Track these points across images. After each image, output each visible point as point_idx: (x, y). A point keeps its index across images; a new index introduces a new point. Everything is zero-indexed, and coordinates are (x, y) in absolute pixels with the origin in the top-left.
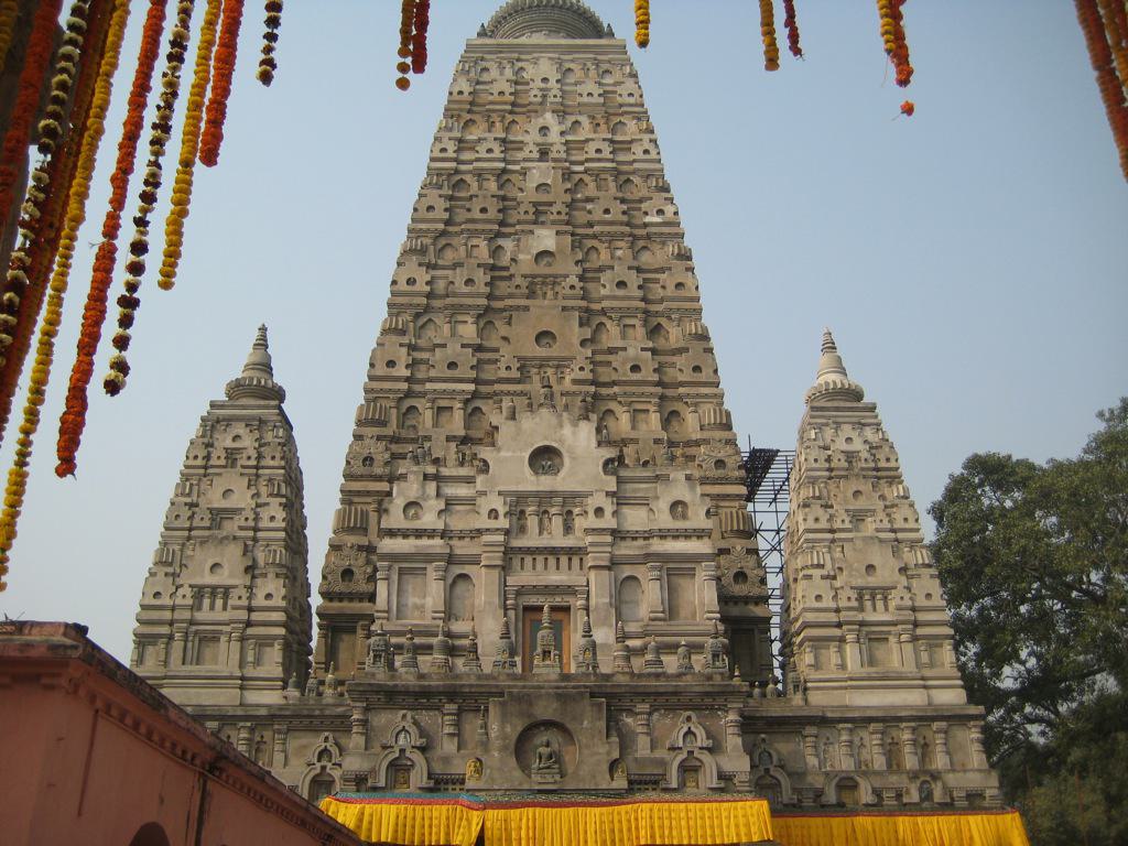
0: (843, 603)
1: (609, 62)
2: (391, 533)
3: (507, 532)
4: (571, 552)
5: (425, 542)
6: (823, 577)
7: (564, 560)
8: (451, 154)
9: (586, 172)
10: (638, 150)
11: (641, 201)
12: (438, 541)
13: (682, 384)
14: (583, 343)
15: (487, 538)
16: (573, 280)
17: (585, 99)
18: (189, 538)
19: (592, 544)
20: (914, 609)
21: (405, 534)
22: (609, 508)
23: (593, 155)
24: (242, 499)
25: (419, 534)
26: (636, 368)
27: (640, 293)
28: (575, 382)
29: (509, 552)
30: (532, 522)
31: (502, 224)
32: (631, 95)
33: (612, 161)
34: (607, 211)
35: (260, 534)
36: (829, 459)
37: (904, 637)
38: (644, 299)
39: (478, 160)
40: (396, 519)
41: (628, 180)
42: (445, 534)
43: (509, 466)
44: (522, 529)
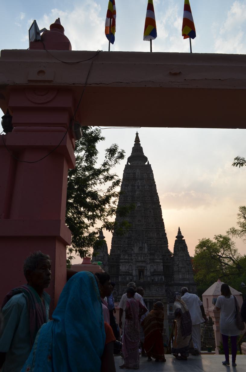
0: (179, 269)
1: (148, 169)
2: (121, 259)
3: (136, 259)
4: (144, 262)
5: (126, 260)
6: (177, 265)
7: (143, 263)
8: (124, 188)
9: (145, 191)
10: (153, 187)
11: (153, 196)
12: (127, 260)
13: (160, 229)
14: (145, 222)
15: (134, 260)
16: (143, 211)
17: (144, 177)
18: (95, 260)
19: (147, 261)
20: (188, 270)
21: (123, 259)
22: (149, 256)
23: (146, 188)
24: (102, 255)
25: (125, 259)
26: (152, 226)
27: (153, 213)
28: (144, 228)
29: (136, 261)
30: (139, 257)
31: (132, 201)
32: (152, 176)
33: (149, 189)
34: (148, 199)
35: (105, 260)
36: (178, 248)
37: (187, 274)
38: (154, 214)
39: (128, 189)
40: (122, 257)
41: (151, 192)
42: (128, 259)
43: (136, 250)
44: (138, 258)
